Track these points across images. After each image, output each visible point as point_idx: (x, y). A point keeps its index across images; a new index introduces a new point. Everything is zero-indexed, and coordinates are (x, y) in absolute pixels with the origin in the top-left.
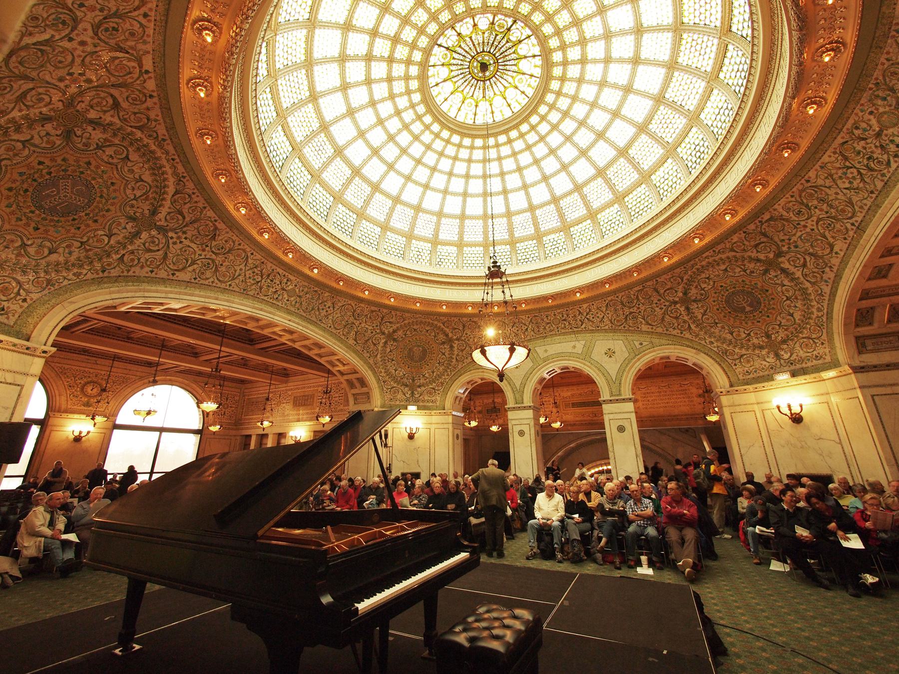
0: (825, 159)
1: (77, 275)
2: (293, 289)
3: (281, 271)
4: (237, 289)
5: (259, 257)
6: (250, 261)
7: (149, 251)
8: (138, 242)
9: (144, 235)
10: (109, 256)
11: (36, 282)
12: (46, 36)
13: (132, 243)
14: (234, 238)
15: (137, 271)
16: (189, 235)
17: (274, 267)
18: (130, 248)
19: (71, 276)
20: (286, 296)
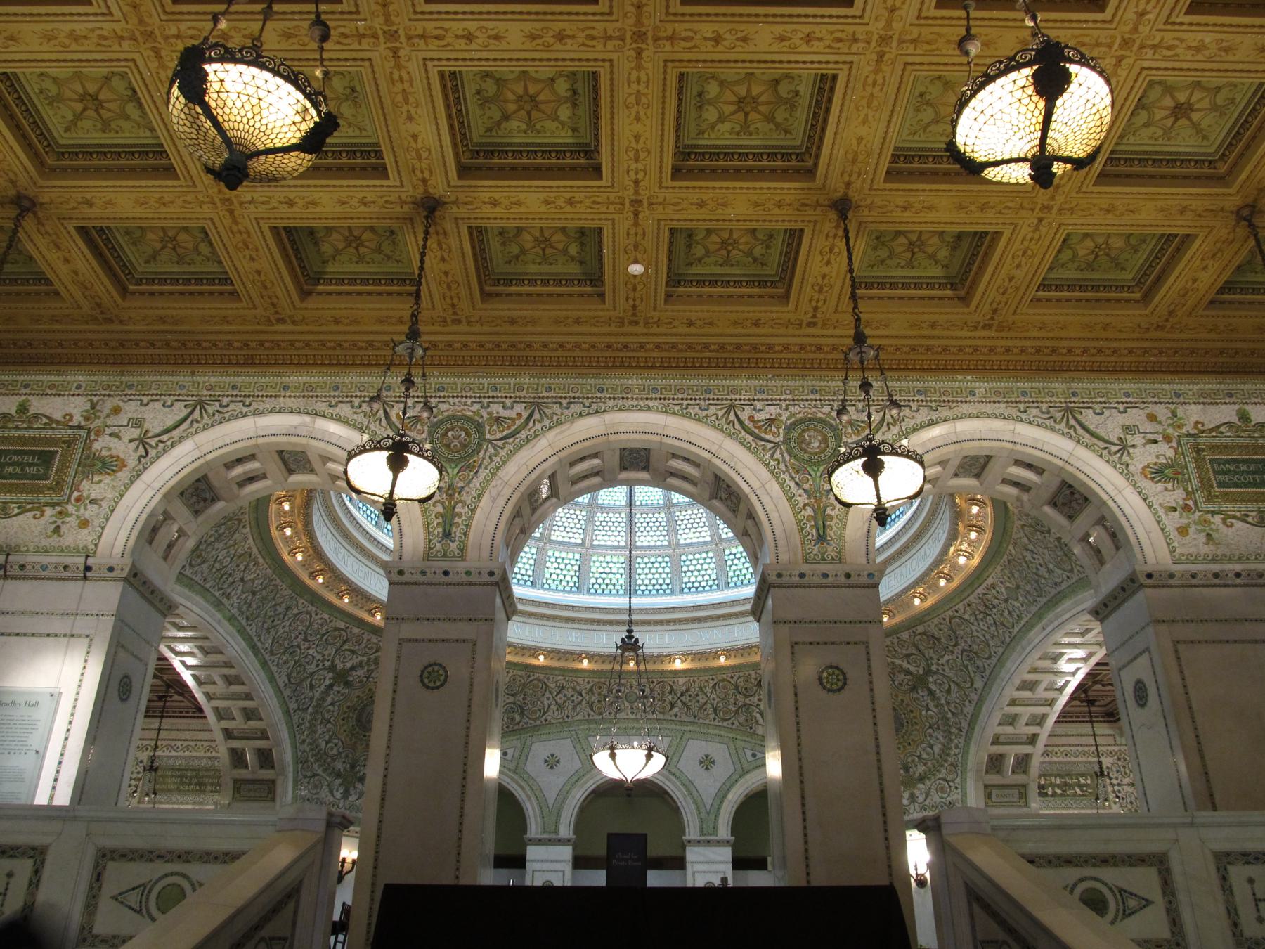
0: (251, 541)
1: (957, 747)
2: (1007, 588)
3: (980, 590)
4: (1001, 650)
5: (961, 606)
6: (966, 616)
7: (948, 691)
8: (938, 694)
9: (933, 687)
10: (948, 719)
11: (950, 772)
12: (758, 716)
13: (938, 699)
14: (936, 621)
15: (969, 709)
16: (935, 657)
17: (975, 594)
18: (943, 701)
19: (957, 751)
20: (1016, 604)
